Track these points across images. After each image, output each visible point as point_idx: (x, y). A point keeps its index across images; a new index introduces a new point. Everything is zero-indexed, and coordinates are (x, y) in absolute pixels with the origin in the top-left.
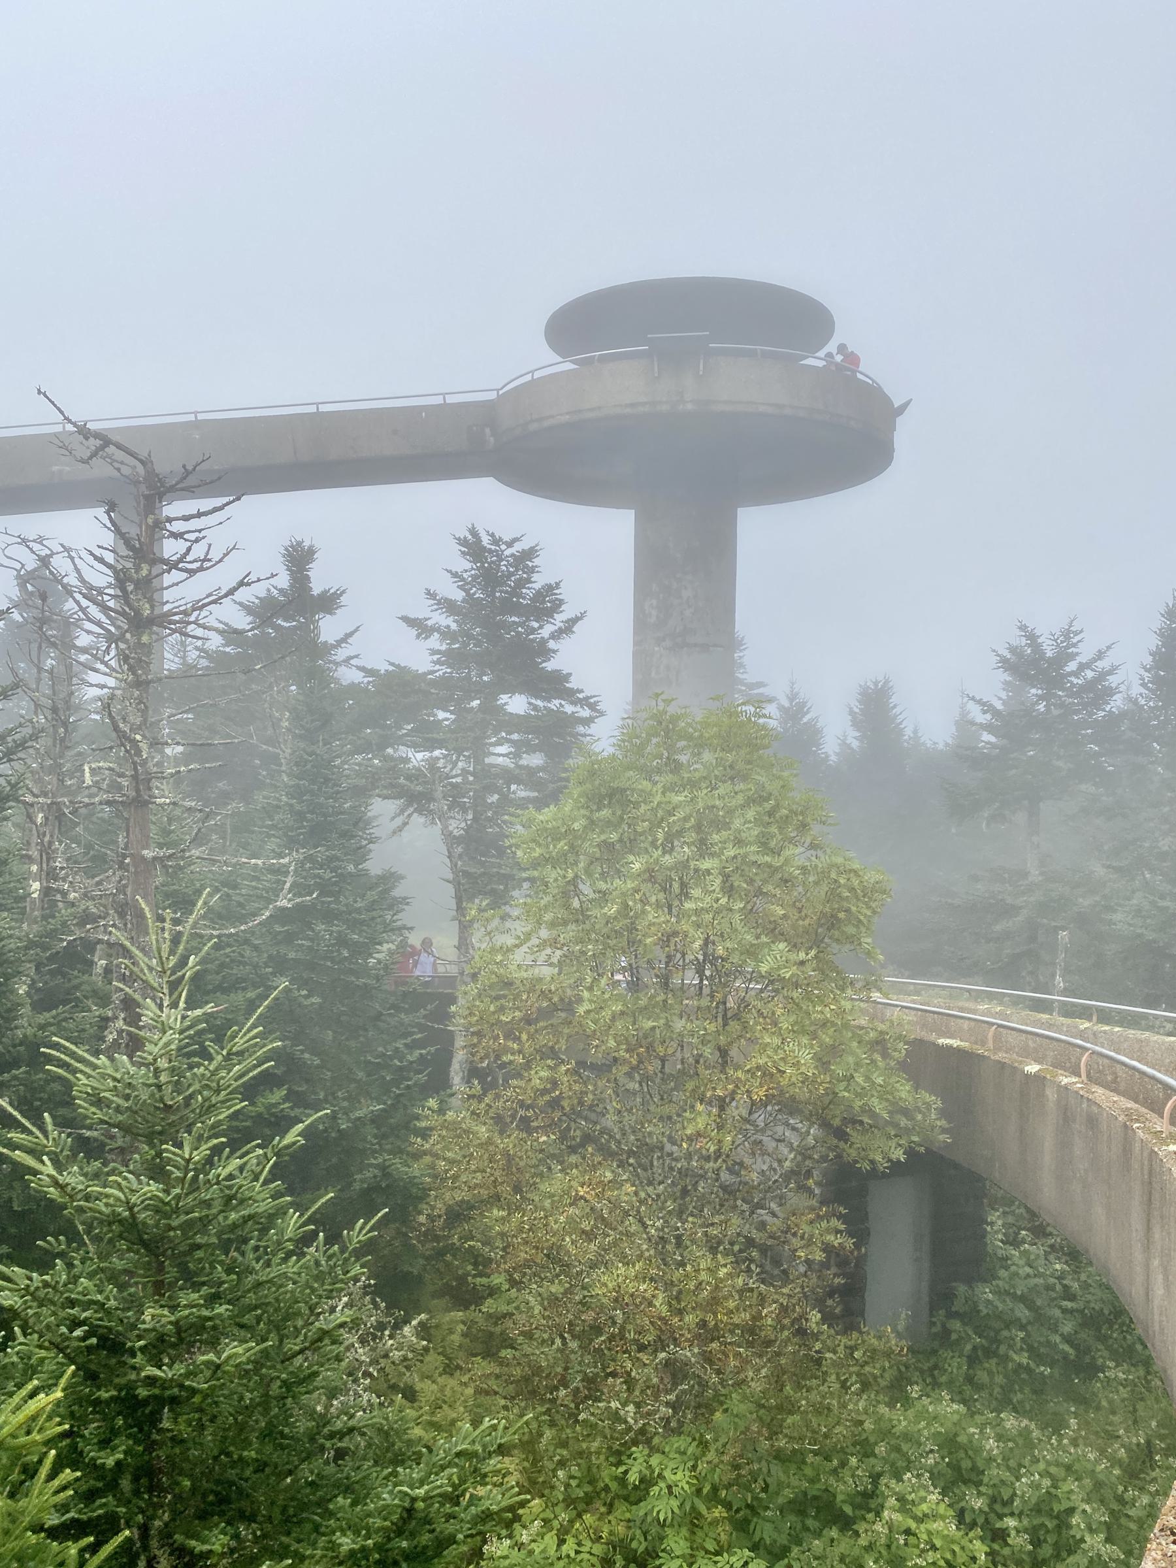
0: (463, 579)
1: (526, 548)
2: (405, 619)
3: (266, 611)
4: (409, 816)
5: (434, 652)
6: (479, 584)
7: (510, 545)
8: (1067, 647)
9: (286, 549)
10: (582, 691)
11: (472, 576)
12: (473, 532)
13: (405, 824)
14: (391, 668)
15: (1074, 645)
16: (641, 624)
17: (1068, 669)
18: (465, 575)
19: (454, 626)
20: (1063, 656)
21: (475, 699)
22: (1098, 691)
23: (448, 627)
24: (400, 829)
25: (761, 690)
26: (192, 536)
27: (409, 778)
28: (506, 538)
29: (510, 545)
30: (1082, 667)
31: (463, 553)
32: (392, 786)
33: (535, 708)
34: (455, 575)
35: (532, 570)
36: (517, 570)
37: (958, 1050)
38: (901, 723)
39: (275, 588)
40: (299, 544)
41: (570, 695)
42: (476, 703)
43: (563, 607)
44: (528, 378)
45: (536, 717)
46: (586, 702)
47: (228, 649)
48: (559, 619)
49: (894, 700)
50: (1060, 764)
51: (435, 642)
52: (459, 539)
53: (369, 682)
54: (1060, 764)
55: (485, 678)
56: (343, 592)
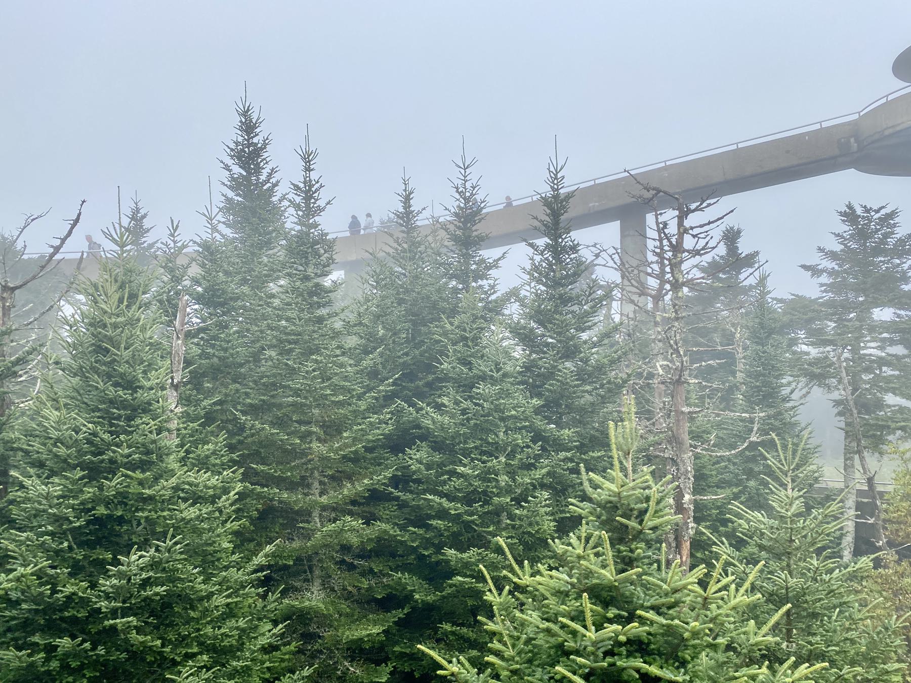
0: (843, 237)
2: (803, 267)
4: (810, 388)
5: (822, 285)
6: (855, 239)
7: (877, 211)
11: (849, 234)
12: (850, 207)
13: (808, 393)
18: (844, 235)
19: (836, 267)
24: (805, 396)
26: (702, 236)
27: (810, 364)
29: (877, 211)
32: (800, 369)
33: (899, 316)
36: (882, 227)
39: (718, 256)
42: (852, 315)
45: (903, 322)
47: (690, 294)
51: (825, 279)
55: (861, 299)
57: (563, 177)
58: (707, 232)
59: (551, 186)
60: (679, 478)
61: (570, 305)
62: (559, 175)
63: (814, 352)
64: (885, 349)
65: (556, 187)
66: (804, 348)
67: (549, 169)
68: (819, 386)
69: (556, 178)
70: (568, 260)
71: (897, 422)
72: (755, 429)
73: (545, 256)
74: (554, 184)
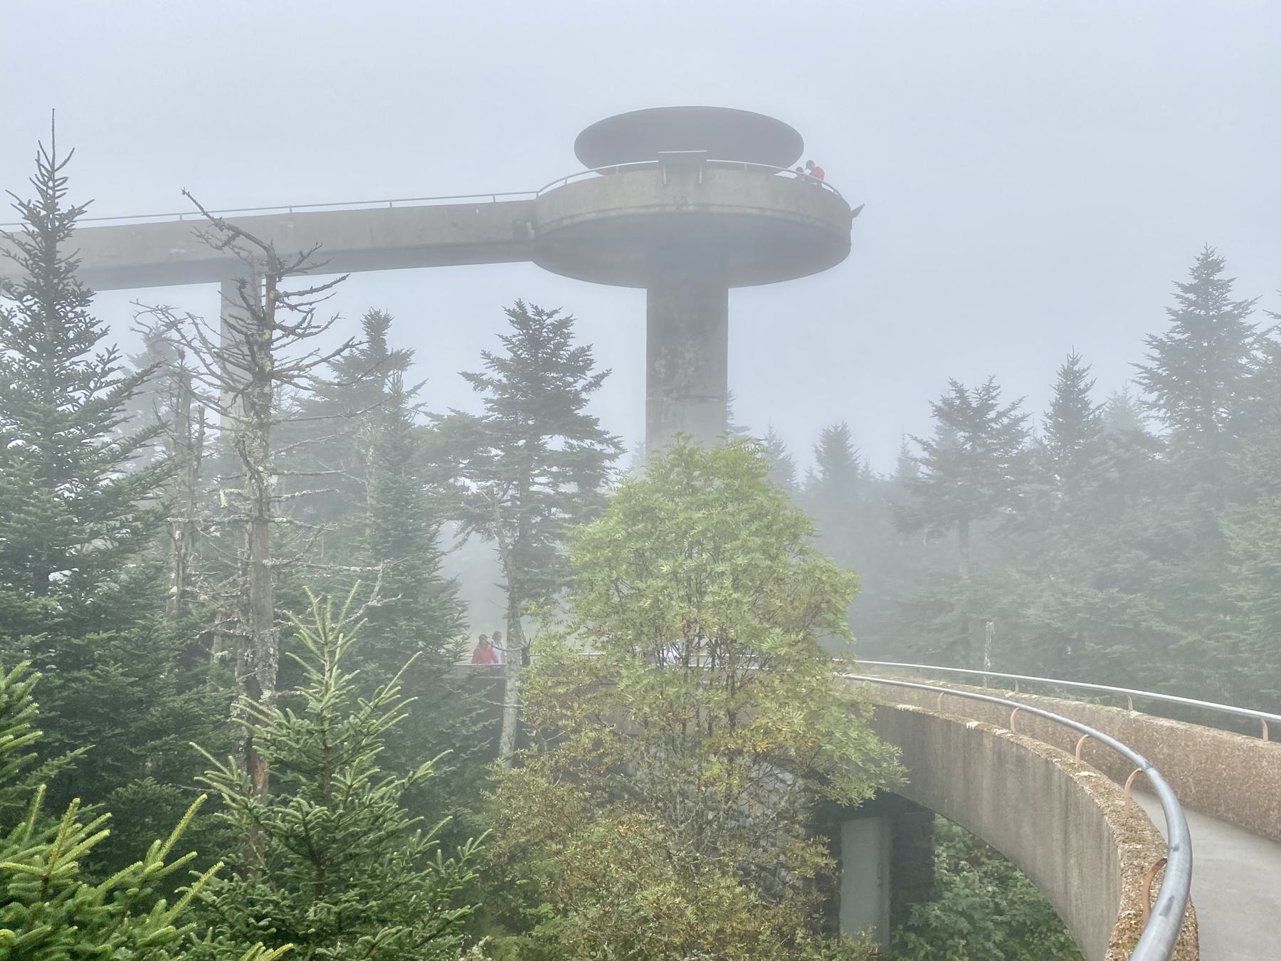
0: (512, 343)
1: (563, 318)
2: (465, 375)
3: (351, 368)
4: (469, 534)
5: (488, 401)
6: (525, 346)
7: (550, 315)
8: (988, 400)
9: (366, 318)
10: (607, 433)
11: (519, 340)
12: (520, 305)
13: (465, 540)
14: (453, 414)
15: (993, 398)
16: (653, 379)
17: (989, 417)
18: (514, 340)
19: (504, 380)
20: (985, 407)
21: (520, 439)
22: (1012, 434)
23: (500, 381)
25: (746, 433)
27: (469, 502)
28: (547, 311)
29: (550, 315)
30: (1000, 415)
31: (512, 321)
32: (455, 509)
33: (571, 446)
34: (505, 339)
35: (568, 336)
36: (556, 336)
37: (914, 713)
38: (856, 460)
40: (377, 313)
41: (598, 436)
42: (521, 442)
43: (593, 366)
44: (562, 183)
45: (572, 453)
46: (611, 442)
47: (317, 399)
48: (590, 375)
49: (849, 442)
50: (984, 490)
51: (489, 393)
52: (509, 311)
53: (434, 426)
54: (984, 490)
55: (530, 422)
56: (412, 352)
57: (66, 179)
58: (311, 304)
59: (41, 191)
60: (256, 666)
61: (70, 389)
62: (58, 175)
63: (474, 487)
64: (558, 486)
65: (50, 192)
66: (468, 482)
67: (38, 161)
68: (478, 531)
69: (51, 178)
70: (71, 315)
71: (563, 576)
72: (377, 589)
73: (26, 304)
74: (48, 188)
